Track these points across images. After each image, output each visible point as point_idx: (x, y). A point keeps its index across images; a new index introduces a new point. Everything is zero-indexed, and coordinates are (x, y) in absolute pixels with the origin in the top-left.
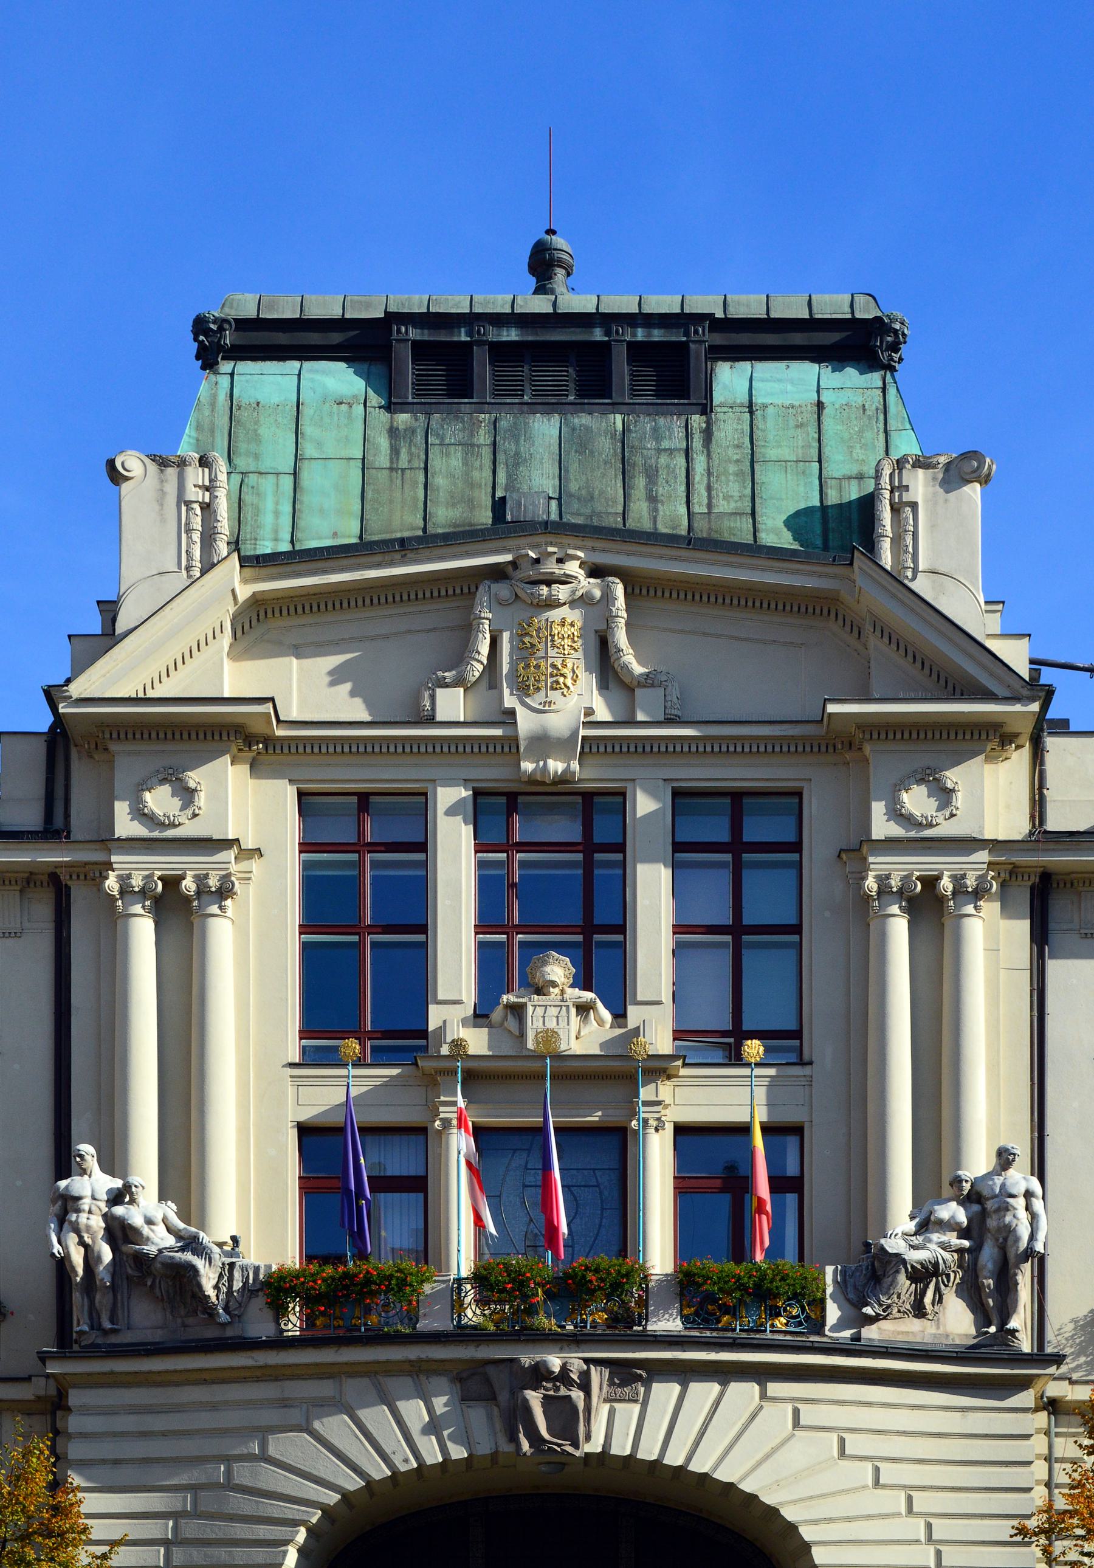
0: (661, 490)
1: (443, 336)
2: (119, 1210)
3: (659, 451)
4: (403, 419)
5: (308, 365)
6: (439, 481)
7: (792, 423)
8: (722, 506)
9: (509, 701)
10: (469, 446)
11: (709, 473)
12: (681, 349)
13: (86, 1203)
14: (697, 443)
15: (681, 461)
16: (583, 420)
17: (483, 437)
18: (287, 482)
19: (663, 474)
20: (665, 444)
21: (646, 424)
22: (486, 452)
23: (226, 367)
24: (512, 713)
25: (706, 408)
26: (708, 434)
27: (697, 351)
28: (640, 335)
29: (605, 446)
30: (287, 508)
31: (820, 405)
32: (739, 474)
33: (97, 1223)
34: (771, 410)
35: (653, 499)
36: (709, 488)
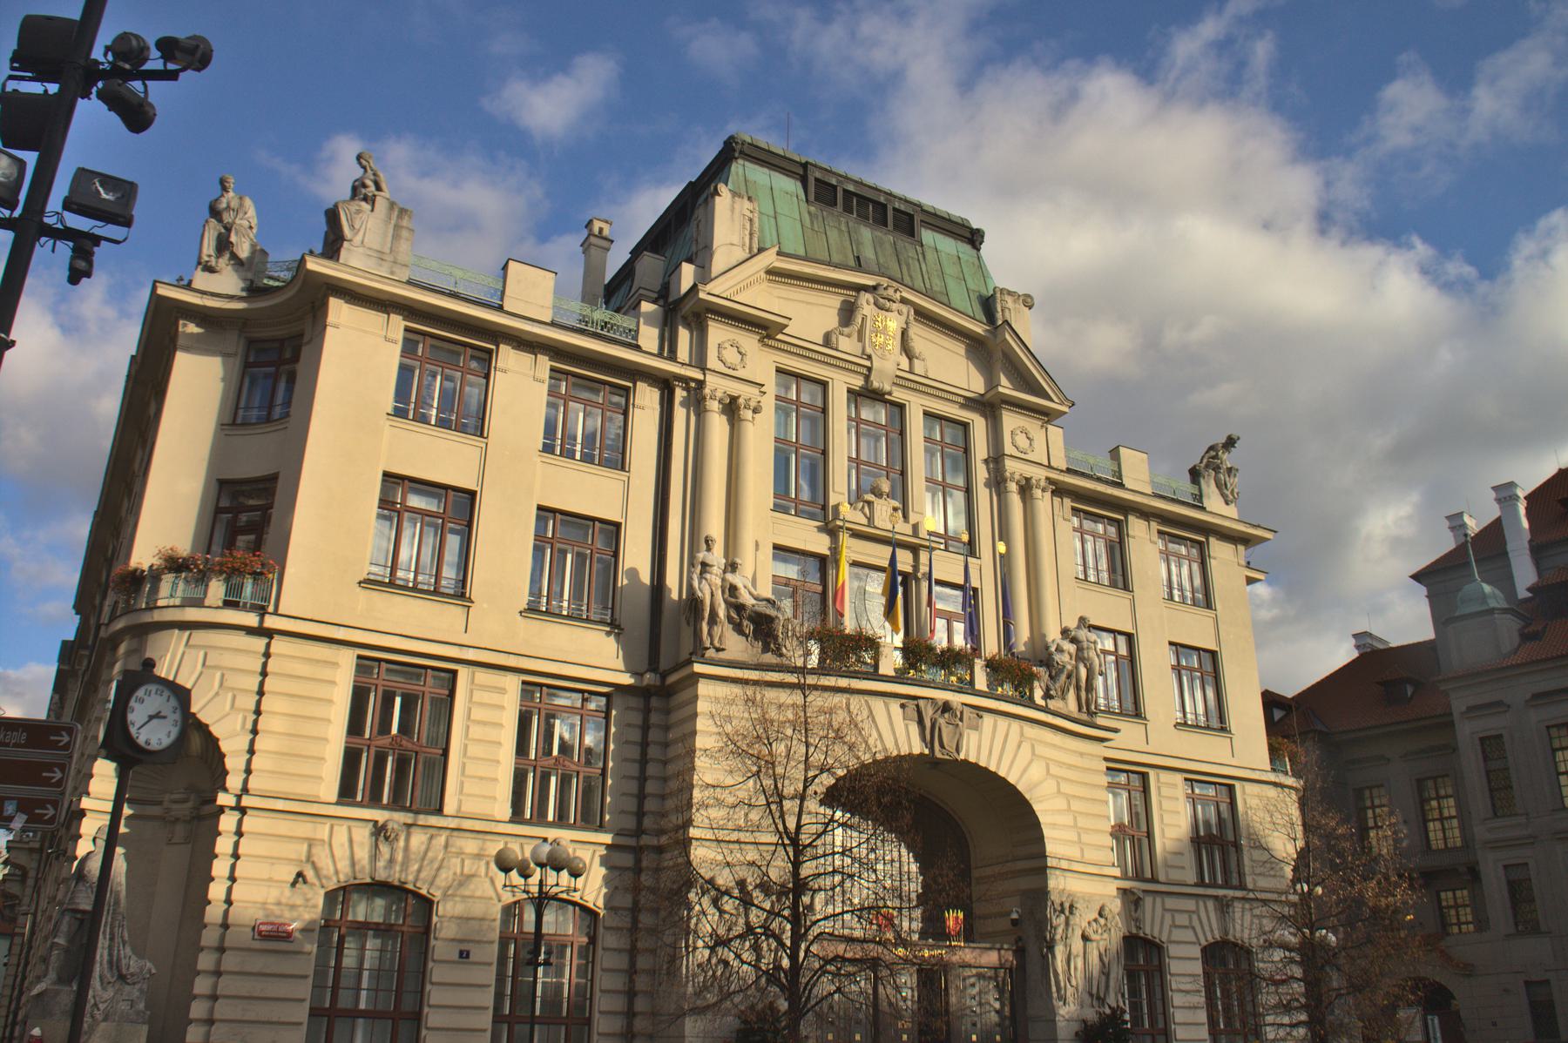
0: (913, 274)
2: (729, 576)
4: (812, 209)
5: (772, 173)
6: (831, 241)
8: (935, 288)
9: (869, 350)
10: (840, 230)
12: (911, 217)
13: (715, 570)
14: (921, 259)
16: (879, 234)
17: (844, 228)
18: (773, 220)
21: (900, 244)
23: (740, 161)
24: (869, 358)
25: (922, 245)
27: (917, 219)
28: (897, 206)
29: (889, 249)
30: (774, 233)
33: (719, 582)
35: (911, 277)
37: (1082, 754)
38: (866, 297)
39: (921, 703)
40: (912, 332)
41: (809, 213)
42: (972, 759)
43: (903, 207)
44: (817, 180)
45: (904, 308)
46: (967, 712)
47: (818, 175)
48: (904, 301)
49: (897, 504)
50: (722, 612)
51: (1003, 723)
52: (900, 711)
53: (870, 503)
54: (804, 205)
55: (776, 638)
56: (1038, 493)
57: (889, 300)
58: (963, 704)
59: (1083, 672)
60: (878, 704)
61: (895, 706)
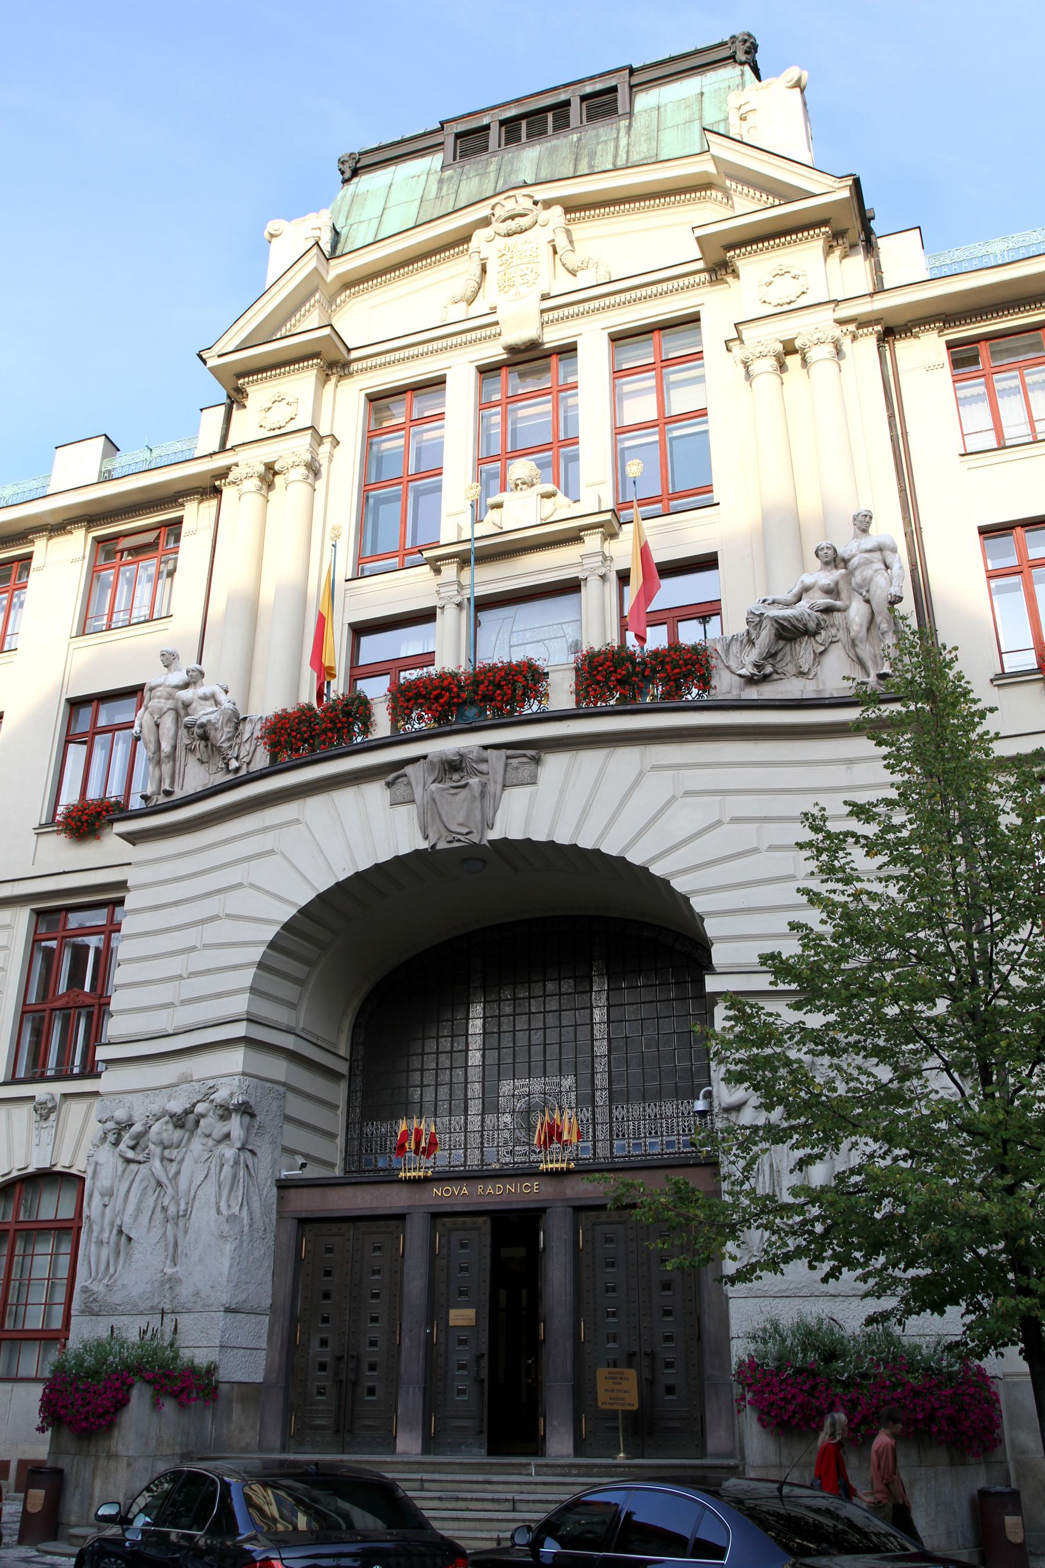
1: (474, 124)
3: (598, 143)
7: (683, 106)
11: (628, 144)
14: (623, 132)
15: (612, 144)
17: (493, 168)
19: (599, 153)
20: (603, 139)
22: (493, 176)
26: (630, 127)
28: (588, 89)
31: (702, 94)
32: (649, 139)
33: (170, 704)
34: (670, 107)
36: (628, 152)
37: (851, 761)
38: (479, 236)
39: (409, 769)
40: (562, 242)
41: (441, 181)
42: (515, 835)
43: (599, 86)
44: (458, 136)
45: (544, 215)
46: (491, 754)
47: (461, 127)
48: (548, 204)
49: (550, 487)
50: (166, 747)
51: (591, 759)
52: (387, 793)
53: (499, 506)
54: (434, 179)
55: (216, 750)
56: (820, 354)
57: (512, 217)
58: (486, 747)
59: (857, 612)
60: (345, 797)
61: (375, 792)
